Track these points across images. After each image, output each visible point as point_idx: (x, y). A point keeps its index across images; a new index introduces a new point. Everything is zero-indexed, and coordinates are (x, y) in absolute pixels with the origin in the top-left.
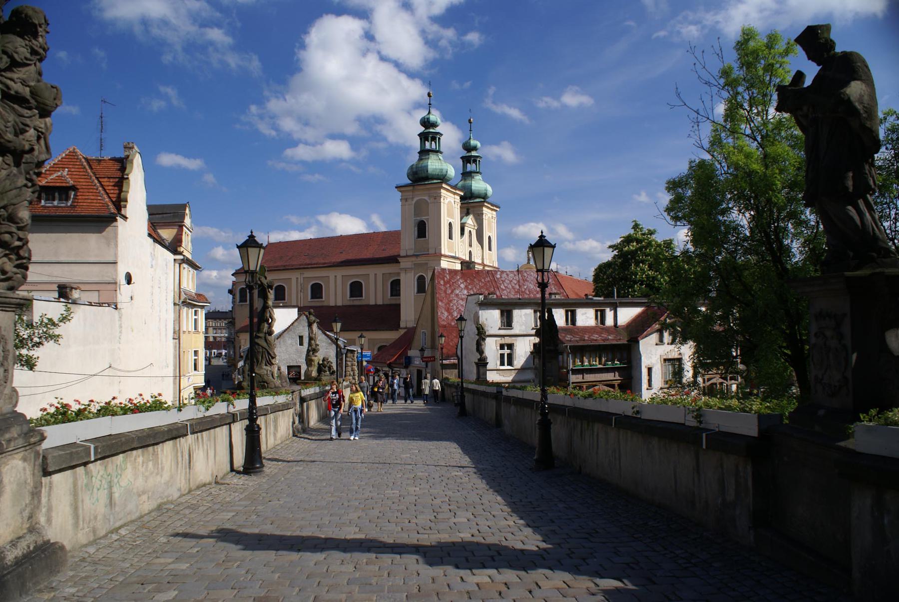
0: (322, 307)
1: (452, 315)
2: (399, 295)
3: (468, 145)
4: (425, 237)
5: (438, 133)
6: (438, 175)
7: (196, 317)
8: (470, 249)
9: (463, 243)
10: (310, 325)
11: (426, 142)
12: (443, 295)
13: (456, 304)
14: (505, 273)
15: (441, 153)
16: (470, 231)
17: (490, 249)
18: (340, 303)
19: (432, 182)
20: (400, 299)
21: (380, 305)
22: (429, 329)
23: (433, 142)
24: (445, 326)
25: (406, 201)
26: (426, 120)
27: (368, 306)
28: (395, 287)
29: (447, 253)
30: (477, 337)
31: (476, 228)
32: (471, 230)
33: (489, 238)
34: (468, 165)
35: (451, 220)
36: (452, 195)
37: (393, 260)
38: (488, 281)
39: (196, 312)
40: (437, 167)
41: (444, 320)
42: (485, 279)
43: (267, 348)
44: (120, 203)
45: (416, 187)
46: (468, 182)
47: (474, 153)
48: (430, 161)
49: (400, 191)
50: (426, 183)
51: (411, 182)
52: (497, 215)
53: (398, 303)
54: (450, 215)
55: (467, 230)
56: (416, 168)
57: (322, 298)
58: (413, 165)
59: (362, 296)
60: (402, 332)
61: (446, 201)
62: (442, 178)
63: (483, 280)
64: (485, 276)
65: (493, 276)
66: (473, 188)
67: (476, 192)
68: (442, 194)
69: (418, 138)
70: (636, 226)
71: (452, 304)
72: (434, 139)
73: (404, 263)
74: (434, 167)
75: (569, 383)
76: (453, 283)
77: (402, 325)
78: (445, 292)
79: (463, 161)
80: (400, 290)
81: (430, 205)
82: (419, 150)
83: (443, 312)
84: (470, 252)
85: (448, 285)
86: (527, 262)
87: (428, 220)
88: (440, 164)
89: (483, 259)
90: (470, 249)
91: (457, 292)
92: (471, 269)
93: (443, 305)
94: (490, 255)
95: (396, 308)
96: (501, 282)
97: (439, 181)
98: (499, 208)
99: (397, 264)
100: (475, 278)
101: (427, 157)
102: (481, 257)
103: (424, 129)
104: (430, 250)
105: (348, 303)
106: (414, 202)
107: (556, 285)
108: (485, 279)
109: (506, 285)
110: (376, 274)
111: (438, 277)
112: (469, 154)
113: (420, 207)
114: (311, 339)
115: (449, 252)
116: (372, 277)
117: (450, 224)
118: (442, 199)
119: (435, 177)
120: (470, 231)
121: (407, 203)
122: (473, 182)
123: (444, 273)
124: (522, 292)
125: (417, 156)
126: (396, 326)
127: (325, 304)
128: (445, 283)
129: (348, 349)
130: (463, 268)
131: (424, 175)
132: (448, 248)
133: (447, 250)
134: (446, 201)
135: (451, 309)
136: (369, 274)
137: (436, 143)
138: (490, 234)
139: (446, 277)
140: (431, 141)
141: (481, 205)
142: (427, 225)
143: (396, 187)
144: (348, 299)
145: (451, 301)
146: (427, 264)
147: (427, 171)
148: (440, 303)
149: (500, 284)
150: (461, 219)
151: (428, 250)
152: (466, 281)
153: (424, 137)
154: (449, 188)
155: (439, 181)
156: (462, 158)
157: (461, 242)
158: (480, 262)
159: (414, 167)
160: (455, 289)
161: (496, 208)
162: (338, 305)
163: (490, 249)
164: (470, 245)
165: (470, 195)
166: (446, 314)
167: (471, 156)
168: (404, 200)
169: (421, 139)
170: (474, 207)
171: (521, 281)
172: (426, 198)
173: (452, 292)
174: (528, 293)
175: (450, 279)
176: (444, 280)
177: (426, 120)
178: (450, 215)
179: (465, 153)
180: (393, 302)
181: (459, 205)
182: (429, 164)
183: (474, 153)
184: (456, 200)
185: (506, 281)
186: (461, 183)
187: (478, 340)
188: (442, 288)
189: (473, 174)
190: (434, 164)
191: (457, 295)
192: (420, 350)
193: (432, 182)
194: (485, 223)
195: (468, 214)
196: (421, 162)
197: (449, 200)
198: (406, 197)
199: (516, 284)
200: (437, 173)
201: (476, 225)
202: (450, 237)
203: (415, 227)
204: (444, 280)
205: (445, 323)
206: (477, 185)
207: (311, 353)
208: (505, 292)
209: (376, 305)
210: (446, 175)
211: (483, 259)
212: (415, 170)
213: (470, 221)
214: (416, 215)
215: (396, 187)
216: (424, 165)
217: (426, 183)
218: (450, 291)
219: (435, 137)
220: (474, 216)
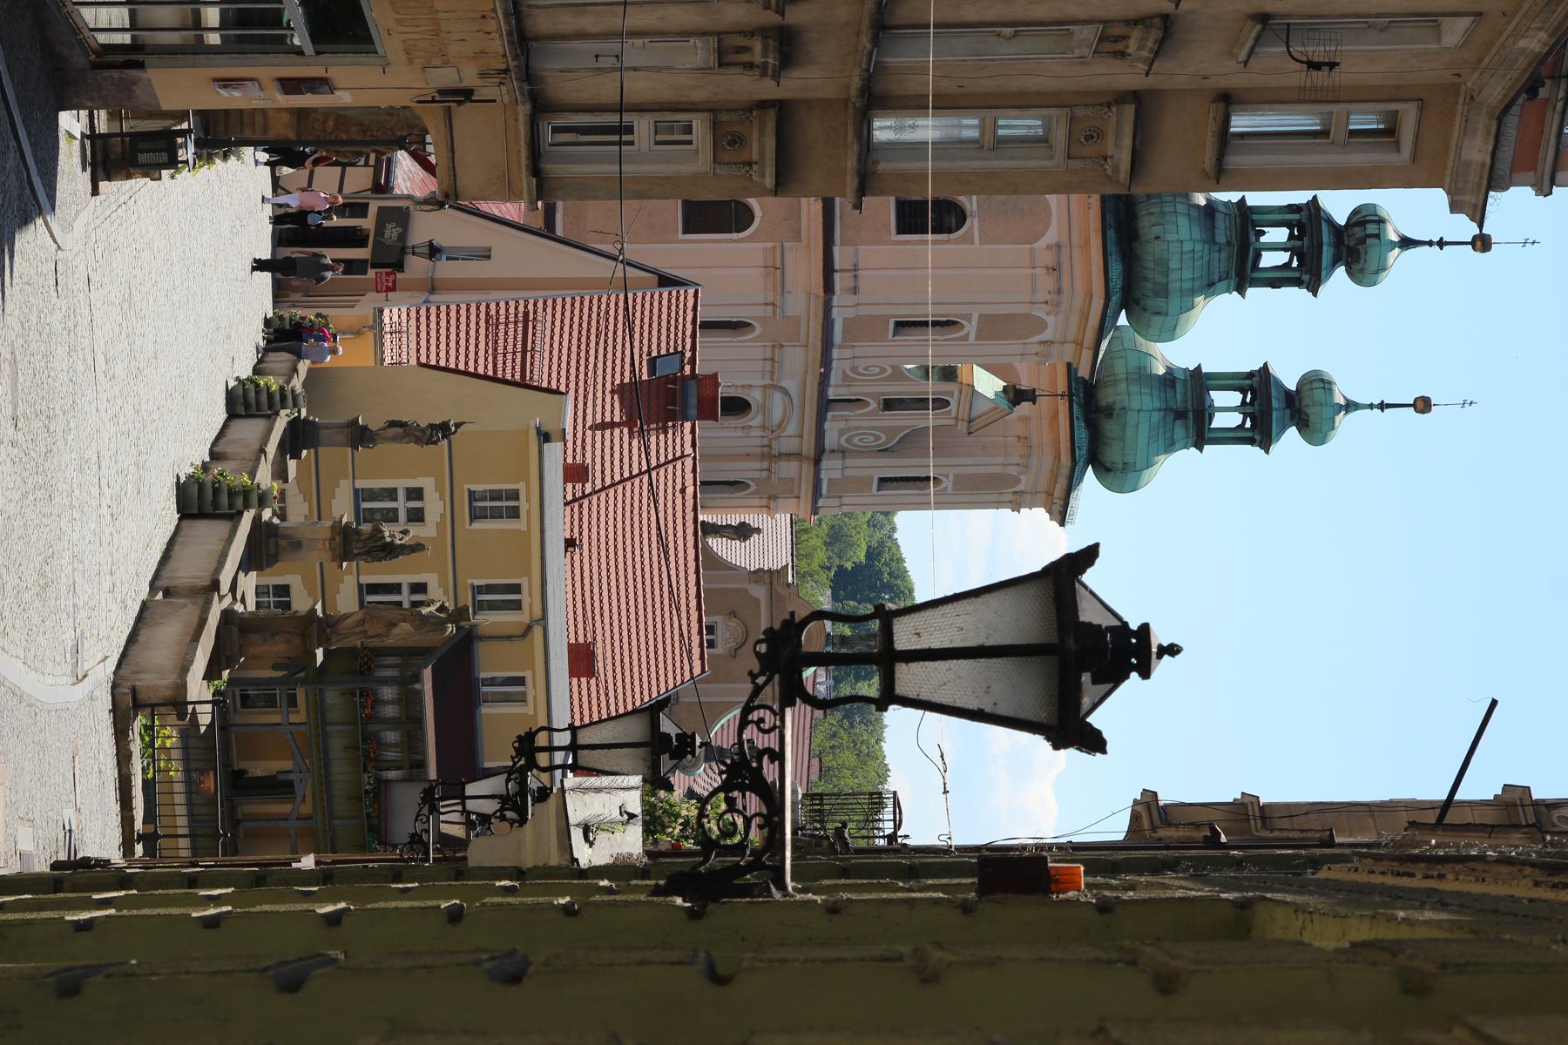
3: (1319, 394)
4: (900, 231)
6: (1146, 279)
8: (873, 405)
9: (891, 378)
15: (1241, 291)
26: (1371, 229)
35: (971, 328)
36: (1071, 336)
40: (1174, 276)
67: (1110, 427)
74: (1174, 264)
79: (1251, 375)
88: (1187, 285)
104: (850, 249)
115: (846, 321)
133: (850, 313)
134: (1040, 312)
146: (796, 236)
164: (889, 404)
165: (1103, 403)
172: (1051, 236)
177: (1371, 229)
197: (1050, 320)
200: (1149, 274)
210: (1145, 310)
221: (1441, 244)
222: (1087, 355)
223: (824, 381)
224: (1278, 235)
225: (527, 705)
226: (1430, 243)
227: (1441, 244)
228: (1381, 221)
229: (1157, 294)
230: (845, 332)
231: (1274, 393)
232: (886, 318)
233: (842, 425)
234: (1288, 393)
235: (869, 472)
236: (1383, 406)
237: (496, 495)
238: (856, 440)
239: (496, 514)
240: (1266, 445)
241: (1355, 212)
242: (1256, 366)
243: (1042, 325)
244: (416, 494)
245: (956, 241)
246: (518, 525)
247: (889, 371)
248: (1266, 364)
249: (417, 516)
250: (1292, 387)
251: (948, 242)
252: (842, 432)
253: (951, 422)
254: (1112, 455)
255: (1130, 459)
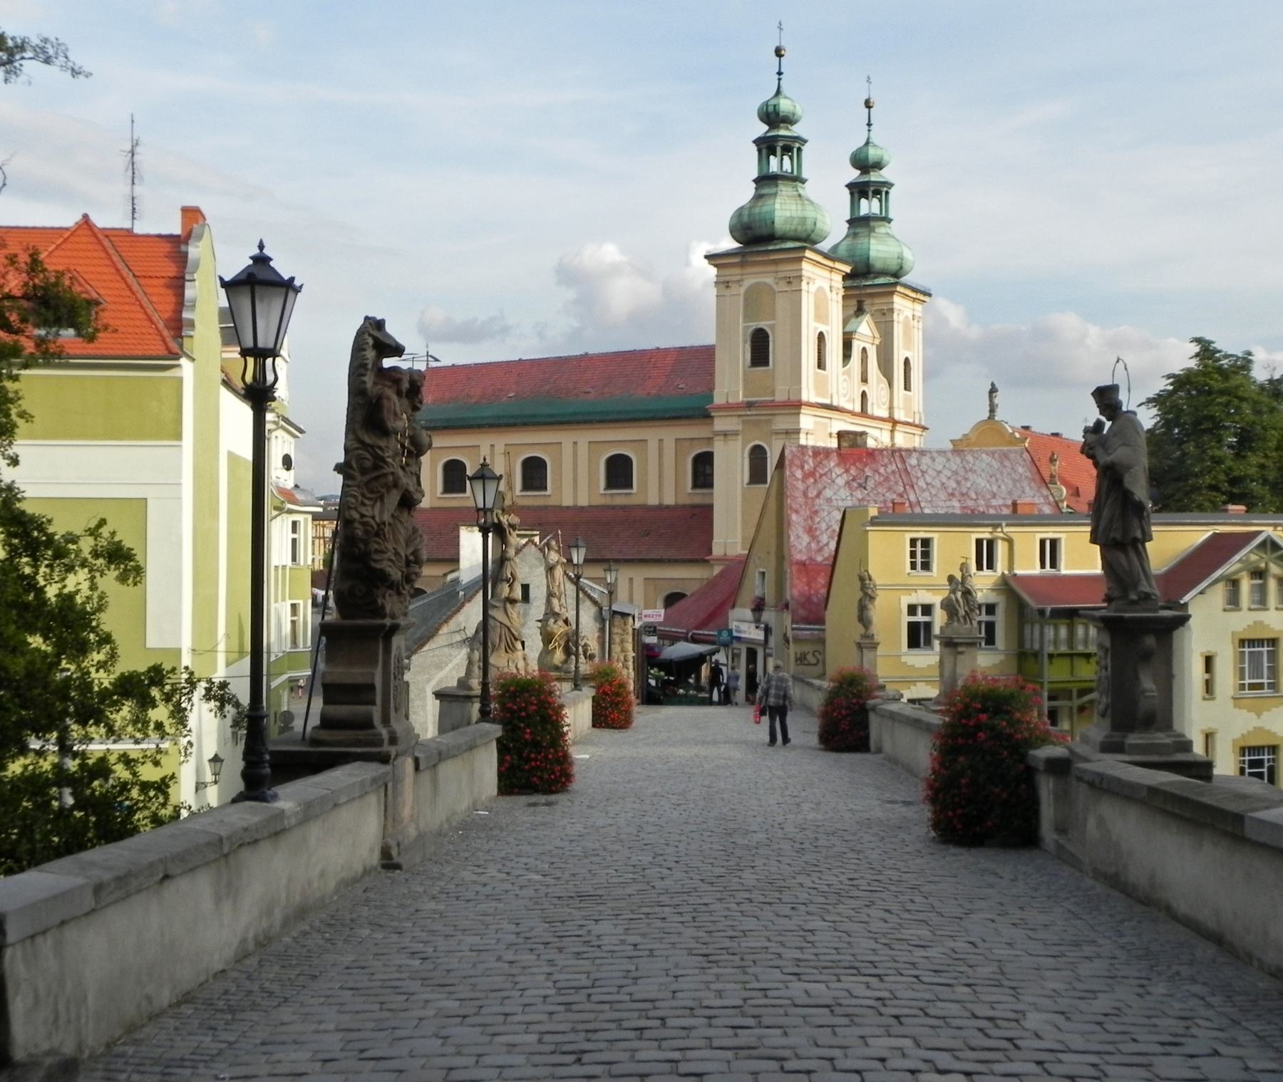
0: (546, 507)
1: (818, 542)
2: (711, 485)
3: (862, 156)
5: (797, 139)
6: (796, 230)
7: (295, 536)
8: (864, 388)
10: (550, 569)
11: (772, 157)
12: (801, 500)
13: (827, 519)
14: (928, 455)
15: (803, 181)
16: (864, 350)
17: (907, 387)
18: (583, 501)
19: (783, 246)
20: (712, 494)
21: (668, 507)
22: (773, 563)
23: (786, 158)
24: (803, 564)
25: (727, 287)
26: (771, 109)
27: (645, 508)
28: (703, 469)
29: (814, 399)
30: (860, 594)
31: (877, 342)
32: (868, 346)
33: (907, 362)
34: (863, 201)
35: (822, 328)
36: (826, 273)
37: (701, 413)
38: (893, 472)
39: (294, 524)
40: (794, 214)
41: (800, 551)
42: (885, 466)
43: (508, 624)
44: (178, 326)
45: (750, 259)
46: (862, 241)
47: (874, 177)
48: (778, 200)
49: (715, 266)
50: (771, 248)
51: (736, 245)
52: (924, 312)
53: (706, 501)
54: (821, 316)
55: (857, 346)
56: (750, 215)
57: (545, 489)
58: (742, 208)
59: (630, 486)
60: (717, 570)
61: (813, 288)
62: (806, 239)
63: (882, 470)
64: (886, 460)
65: (903, 462)
66: (873, 254)
67: (878, 265)
68: (804, 273)
69: (754, 148)
70: (1206, 350)
71: (817, 520)
72: (787, 150)
73: (720, 424)
74: (788, 214)
75: (1042, 683)
76: (821, 476)
77: (717, 551)
78: (805, 494)
79: (852, 194)
80: (712, 475)
81: (778, 296)
82: (755, 175)
83: (801, 534)
84: (864, 395)
85: (812, 480)
86: (987, 414)
87: (772, 327)
89: (891, 408)
90: (864, 388)
91: (828, 493)
92: (858, 446)
93: (801, 520)
94: (908, 400)
95: (701, 517)
96: (919, 474)
97: (798, 244)
98: (930, 295)
99: (708, 421)
100: (866, 465)
101: (772, 190)
102: (887, 405)
103: (766, 128)
105: (598, 501)
106: (742, 291)
107: (1034, 480)
108: (885, 466)
109: (929, 480)
110: (661, 440)
111: (792, 462)
112: (865, 179)
113: (754, 300)
114: (550, 595)
115: (818, 394)
116: (653, 446)
117: (821, 337)
118: (804, 284)
119: (792, 234)
120: (864, 350)
121: (728, 292)
122: (873, 241)
123: (803, 454)
124: (963, 495)
125: (749, 191)
126: (701, 555)
127: (552, 502)
128: (806, 476)
129: (615, 612)
130: (844, 444)
131: (765, 231)
132: (816, 388)
133: (812, 393)
134: (813, 288)
135: (816, 529)
136: (646, 441)
137: (791, 158)
138: (908, 354)
139: (808, 463)
140: (782, 155)
141: (889, 290)
142: (771, 339)
143: (706, 257)
144: (602, 491)
145: (816, 512)
147: (773, 223)
148: (794, 517)
149: (918, 478)
150: (846, 321)
151: (773, 394)
152: (847, 471)
153: (766, 146)
154: (819, 258)
155: (798, 244)
156: (850, 186)
157: (844, 373)
158: (885, 414)
159: (746, 212)
160: (825, 488)
161: (922, 297)
162: (579, 504)
163: (907, 387)
164: (864, 380)
166: (806, 539)
167: (867, 184)
168: (723, 284)
169: (760, 151)
170: (872, 295)
171: (962, 472)
172: (769, 280)
173: (818, 495)
174: (974, 497)
175: (815, 468)
176: (802, 467)
177: (771, 109)
178: (821, 316)
179: (854, 175)
180: (698, 500)
181: (842, 292)
182: (777, 206)
183: (874, 177)
184: (834, 284)
185: (930, 471)
186: (844, 243)
187: (860, 600)
188: (800, 485)
189: (872, 224)
190: (788, 207)
191: (829, 500)
192: (753, 610)
193: (783, 246)
194: (898, 330)
195: (860, 311)
196: (760, 204)
198: (727, 279)
199: (949, 478)
200: (793, 227)
201: (877, 335)
202: (821, 364)
203: (745, 342)
204: (802, 467)
205: (804, 558)
206: (881, 247)
207: (552, 620)
208: (926, 494)
209: (660, 508)
210: (813, 231)
211: (891, 408)
212: (745, 219)
213: (865, 329)
214: (747, 317)
215: (706, 257)
216: (765, 209)
217: (771, 248)
218: (815, 493)
219: (791, 147)
220: (872, 315)
221: (780, 73)
222: (838, 265)
223: (853, 413)
224: (774, 161)
225: (1059, 539)
226: (779, 79)
227: (780, 73)
228: (766, 104)
229: (804, 224)
230: (824, 396)
231: (862, 180)
232: (816, 374)
233: (875, 407)
234: (861, 174)
235: (901, 395)
236: (869, 125)
237: (913, 554)
238: (884, 400)
239: (926, 554)
240: (889, 185)
241: (762, 119)
242: (847, 191)
243: (820, 289)
244: (912, 610)
245: (773, 334)
246: (935, 536)
247: (845, 377)
248: (847, 186)
249: (927, 609)
250: (858, 172)
251: (774, 337)
252: (879, 407)
253: (875, 347)
254: (893, 266)
255: (896, 255)
